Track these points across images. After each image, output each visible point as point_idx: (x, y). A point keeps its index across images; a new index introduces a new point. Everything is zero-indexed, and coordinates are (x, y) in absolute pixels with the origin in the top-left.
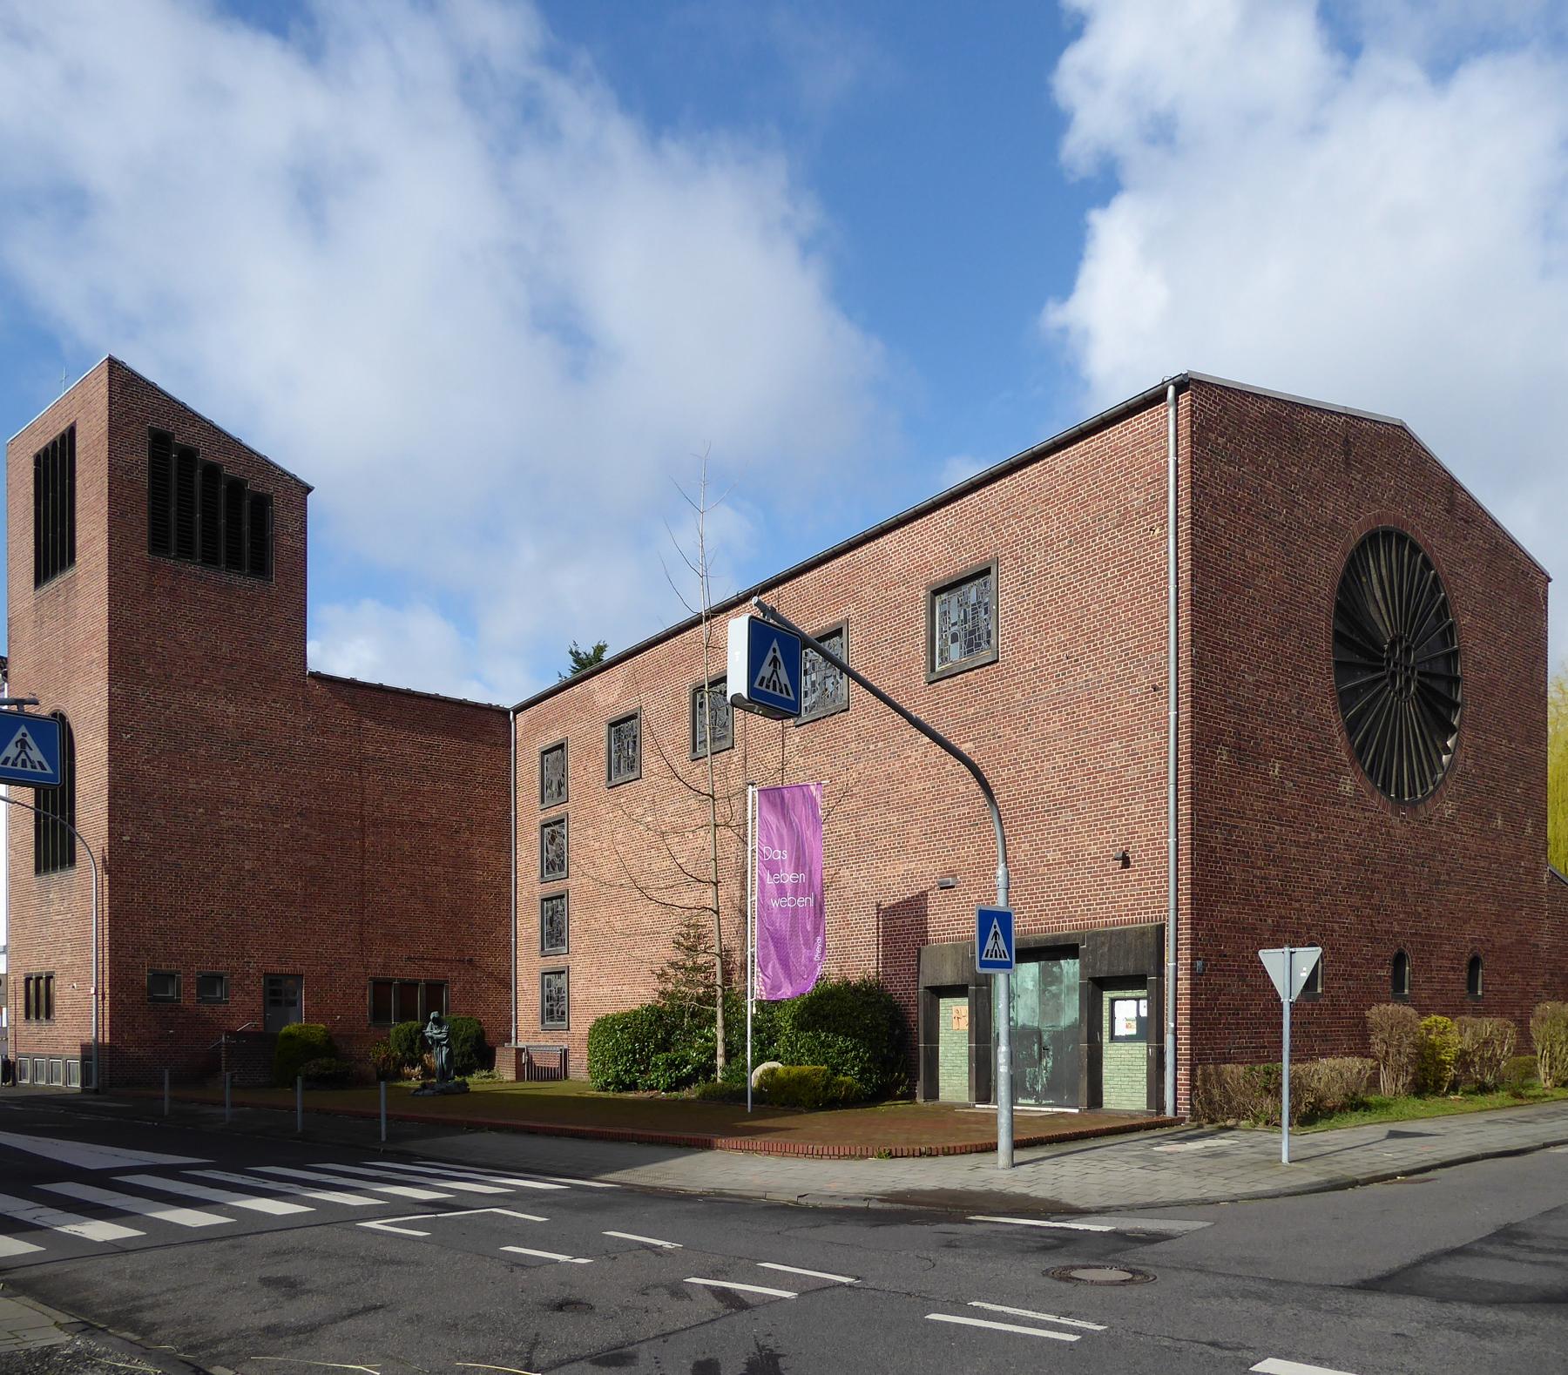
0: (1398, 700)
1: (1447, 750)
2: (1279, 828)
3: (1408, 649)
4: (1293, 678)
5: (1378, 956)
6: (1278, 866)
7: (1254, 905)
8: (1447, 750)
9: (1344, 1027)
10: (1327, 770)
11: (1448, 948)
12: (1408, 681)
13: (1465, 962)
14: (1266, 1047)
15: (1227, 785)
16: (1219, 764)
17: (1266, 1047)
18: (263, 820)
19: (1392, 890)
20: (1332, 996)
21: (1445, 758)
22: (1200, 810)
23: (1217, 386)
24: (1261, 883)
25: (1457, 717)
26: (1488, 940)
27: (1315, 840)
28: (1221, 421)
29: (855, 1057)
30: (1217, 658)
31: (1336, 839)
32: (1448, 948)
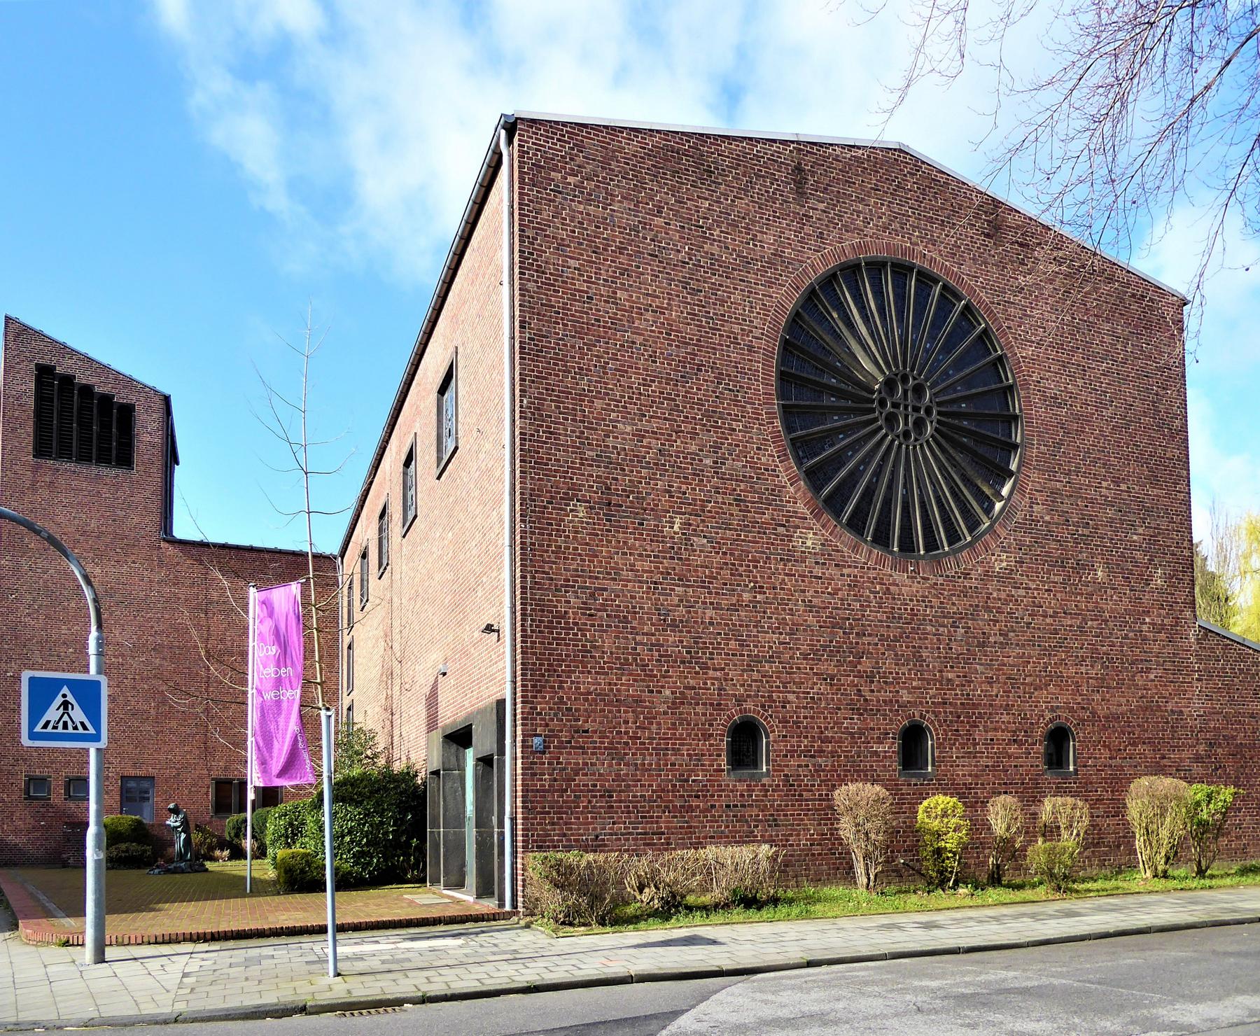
0: (900, 445)
1: (1001, 498)
2: (681, 589)
3: (919, 390)
4: (704, 425)
5: (873, 729)
6: (682, 632)
7: (639, 675)
8: (1001, 498)
9: (809, 810)
10: (771, 524)
11: (1005, 718)
12: (919, 424)
13: (1039, 733)
14: (663, 833)
15: (587, 544)
16: (571, 521)
17: (663, 833)
18: (123, 655)
19: (896, 655)
20: (786, 775)
21: (998, 506)
22: (536, 572)
23: (564, 124)
24: (651, 650)
25: (1017, 459)
26: (1083, 708)
27: (750, 601)
28: (572, 159)
29: (352, 841)
30: (565, 408)
31: (789, 600)
32: (1005, 718)
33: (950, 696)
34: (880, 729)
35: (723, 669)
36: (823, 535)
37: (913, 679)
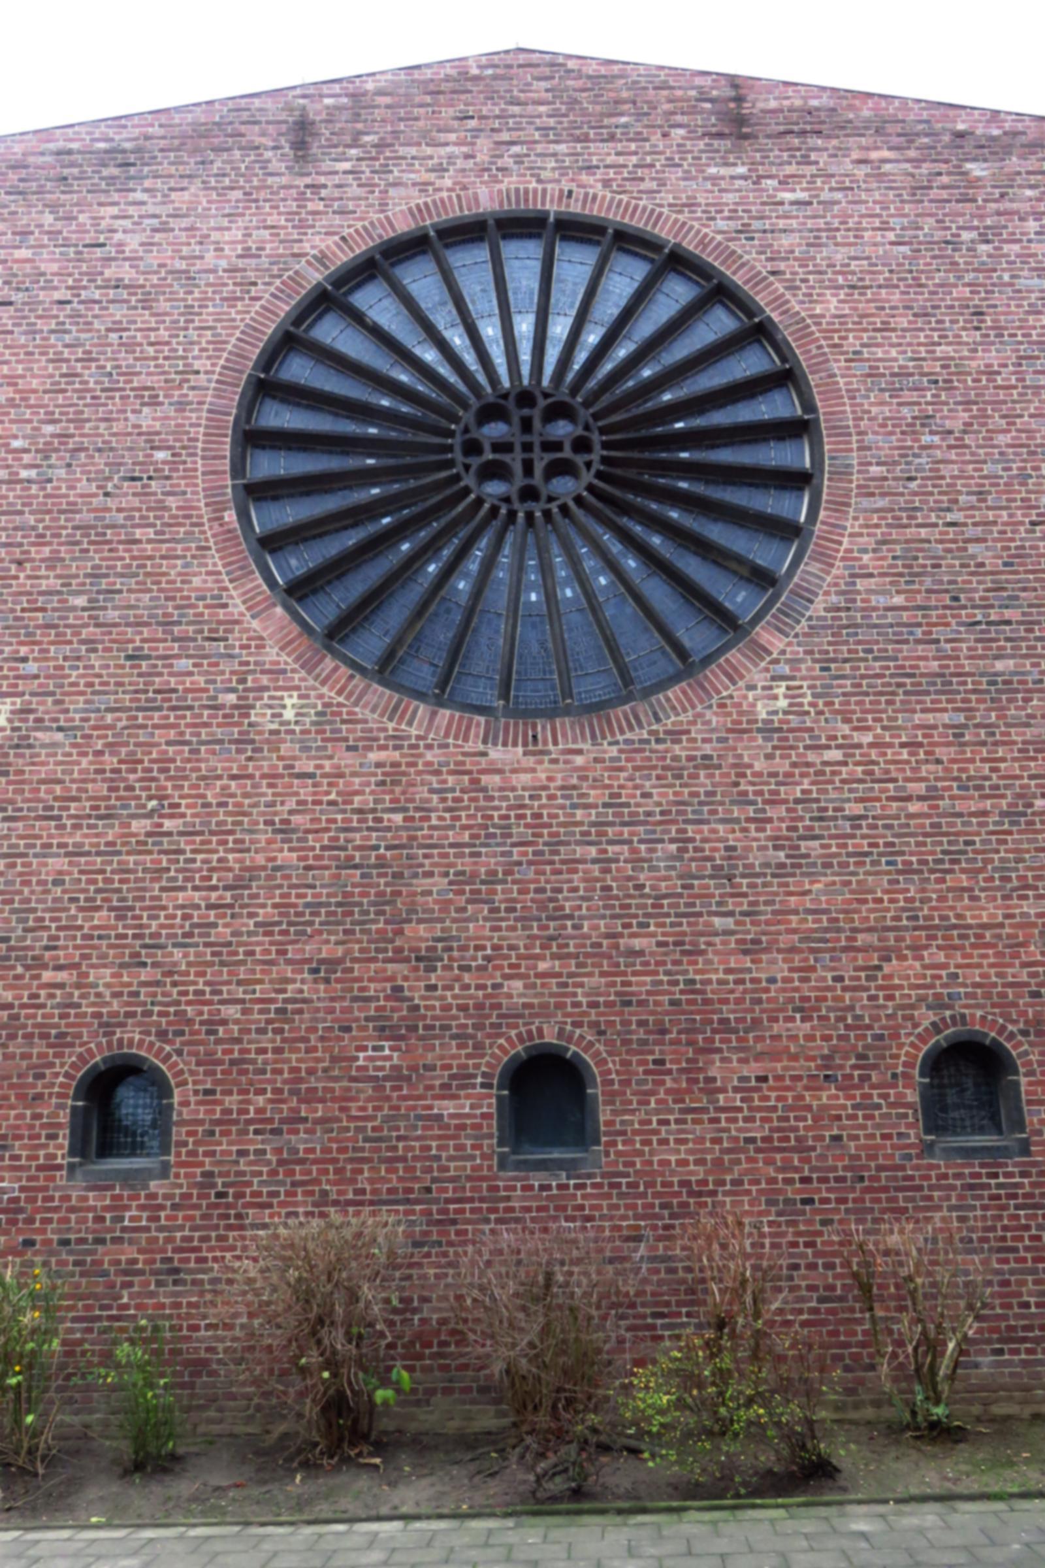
33: (641, 984)
34: (448, 1067)
35: (76, 966)
36: (321, 697)
37: (541, 957)
